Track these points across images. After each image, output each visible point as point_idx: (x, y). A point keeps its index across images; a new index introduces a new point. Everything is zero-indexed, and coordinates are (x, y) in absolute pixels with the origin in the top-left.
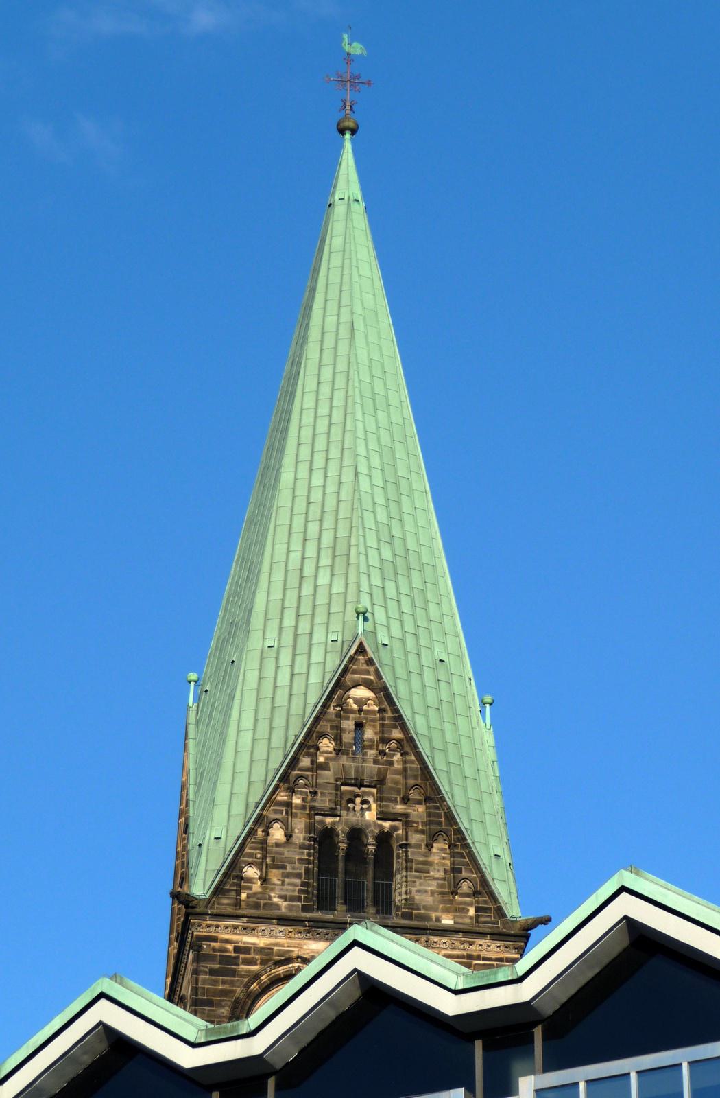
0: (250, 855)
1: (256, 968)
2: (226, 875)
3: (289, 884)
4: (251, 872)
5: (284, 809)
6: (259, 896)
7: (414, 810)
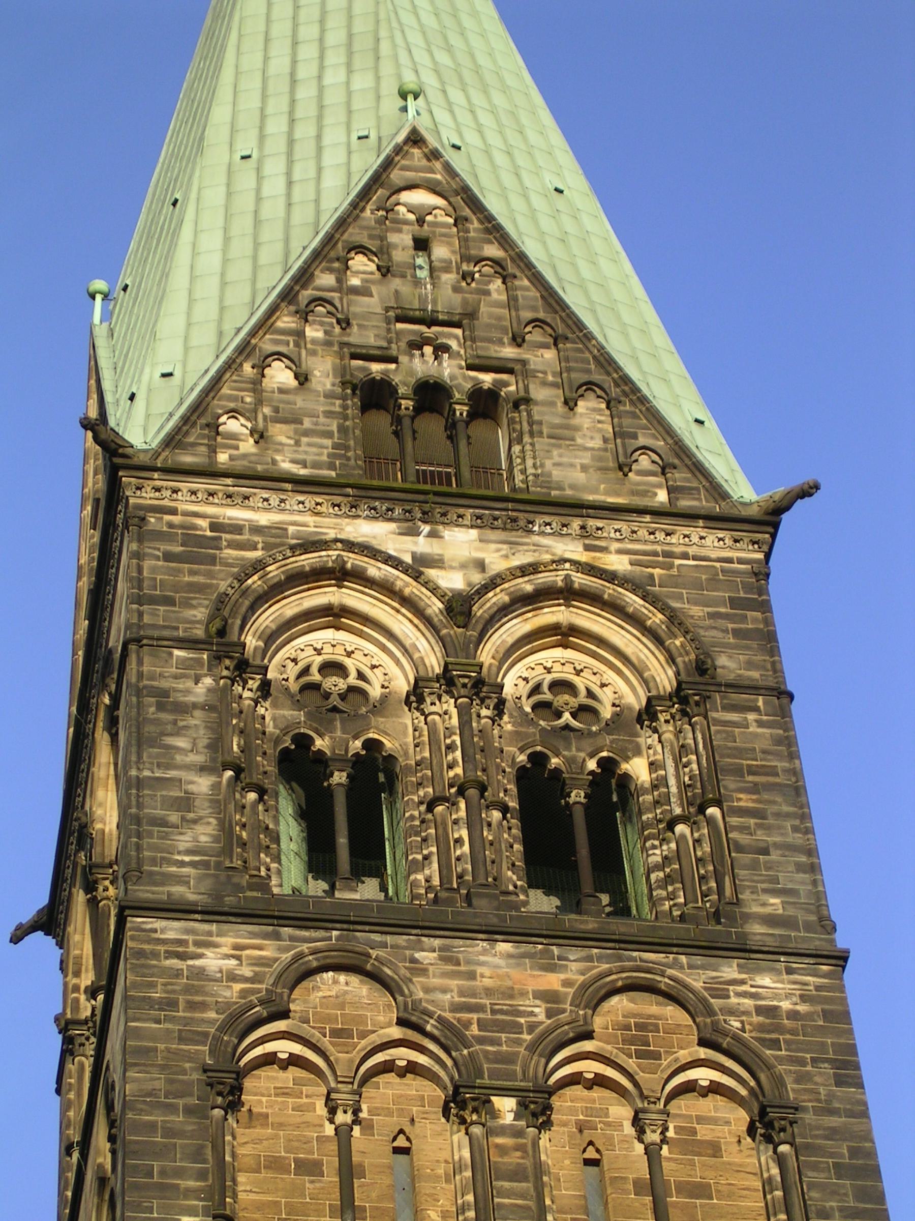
3: (309, 445)
5: (291, 339)
6: (253, 458)
7: (537, 356)
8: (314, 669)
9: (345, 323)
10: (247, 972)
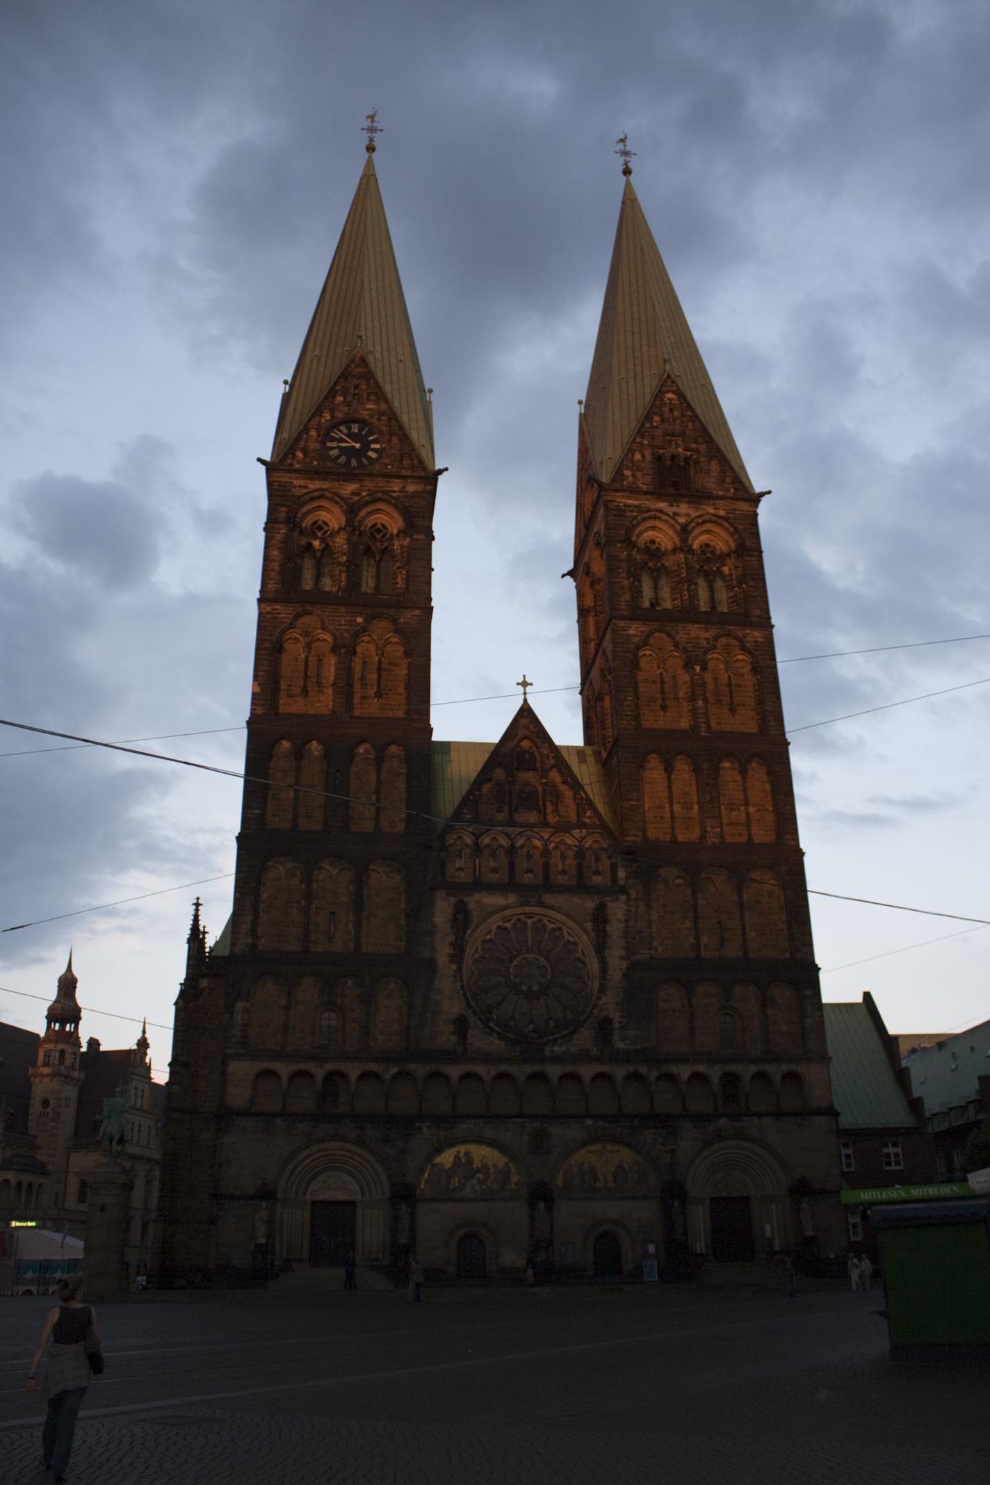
0: (627, 465)
1: (635, 514)
2: (616, 473)
4: (627, 473)
8: (648, 543)
9: (653, 439)
10: (639, 634)
